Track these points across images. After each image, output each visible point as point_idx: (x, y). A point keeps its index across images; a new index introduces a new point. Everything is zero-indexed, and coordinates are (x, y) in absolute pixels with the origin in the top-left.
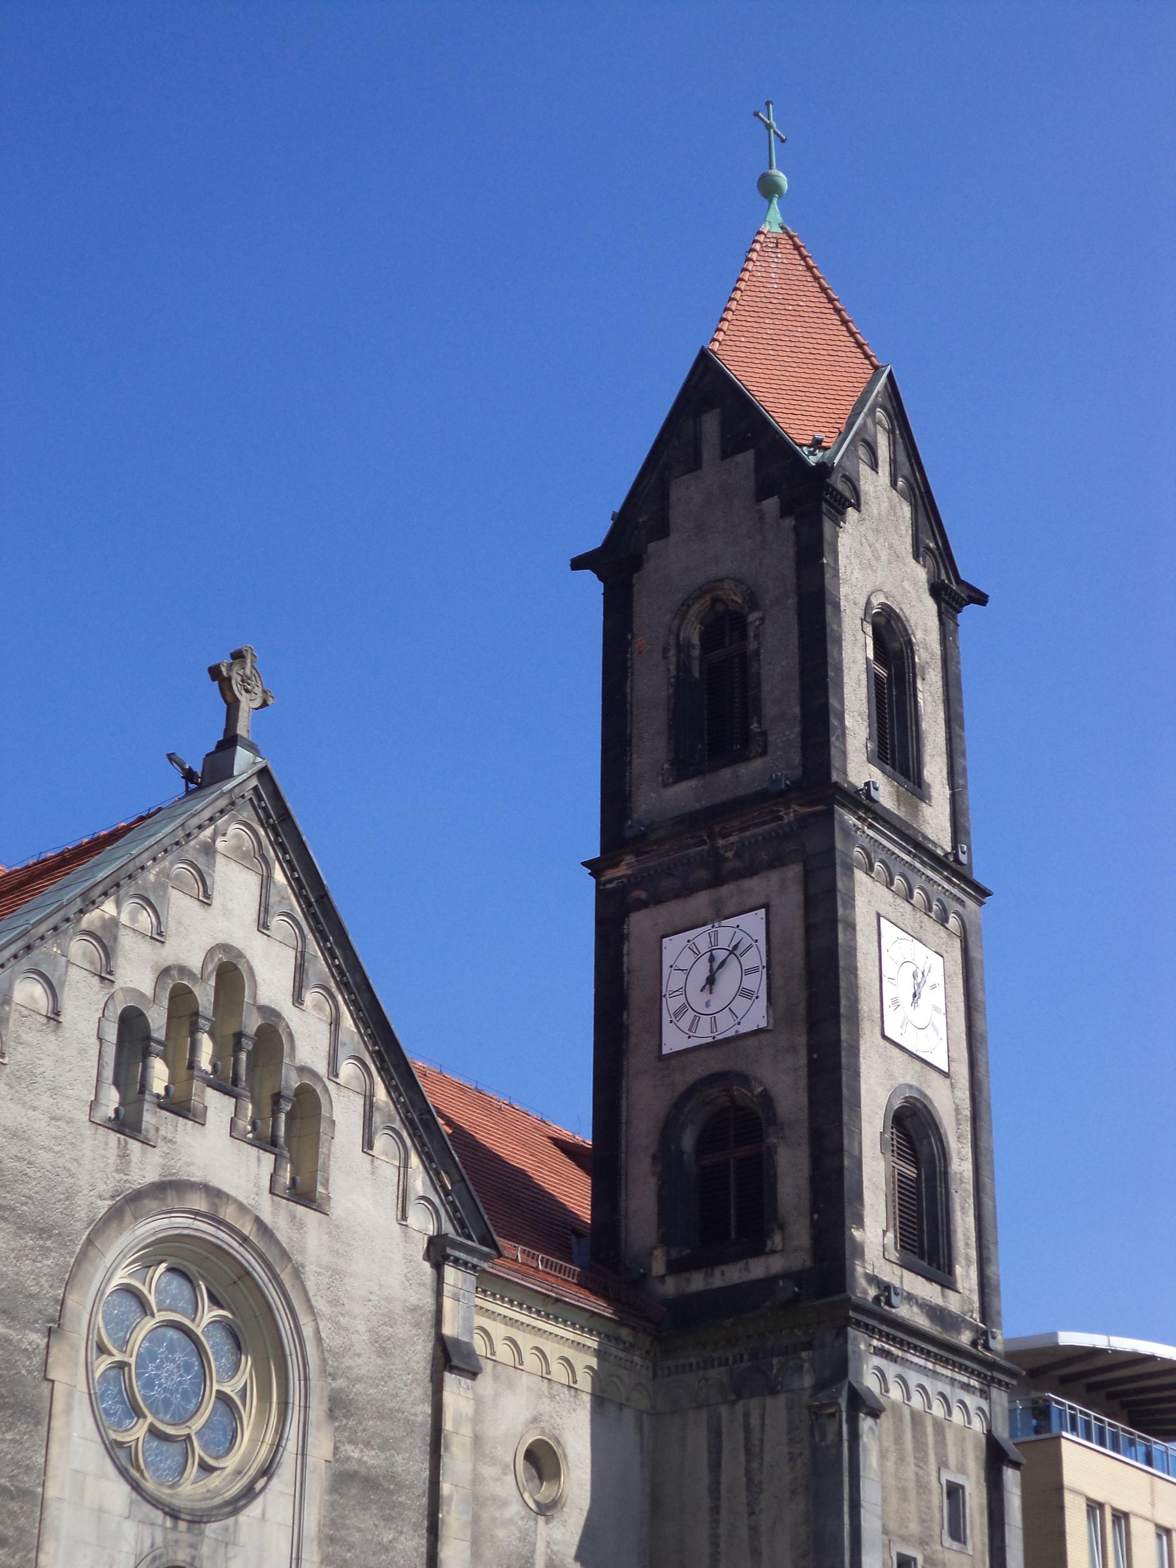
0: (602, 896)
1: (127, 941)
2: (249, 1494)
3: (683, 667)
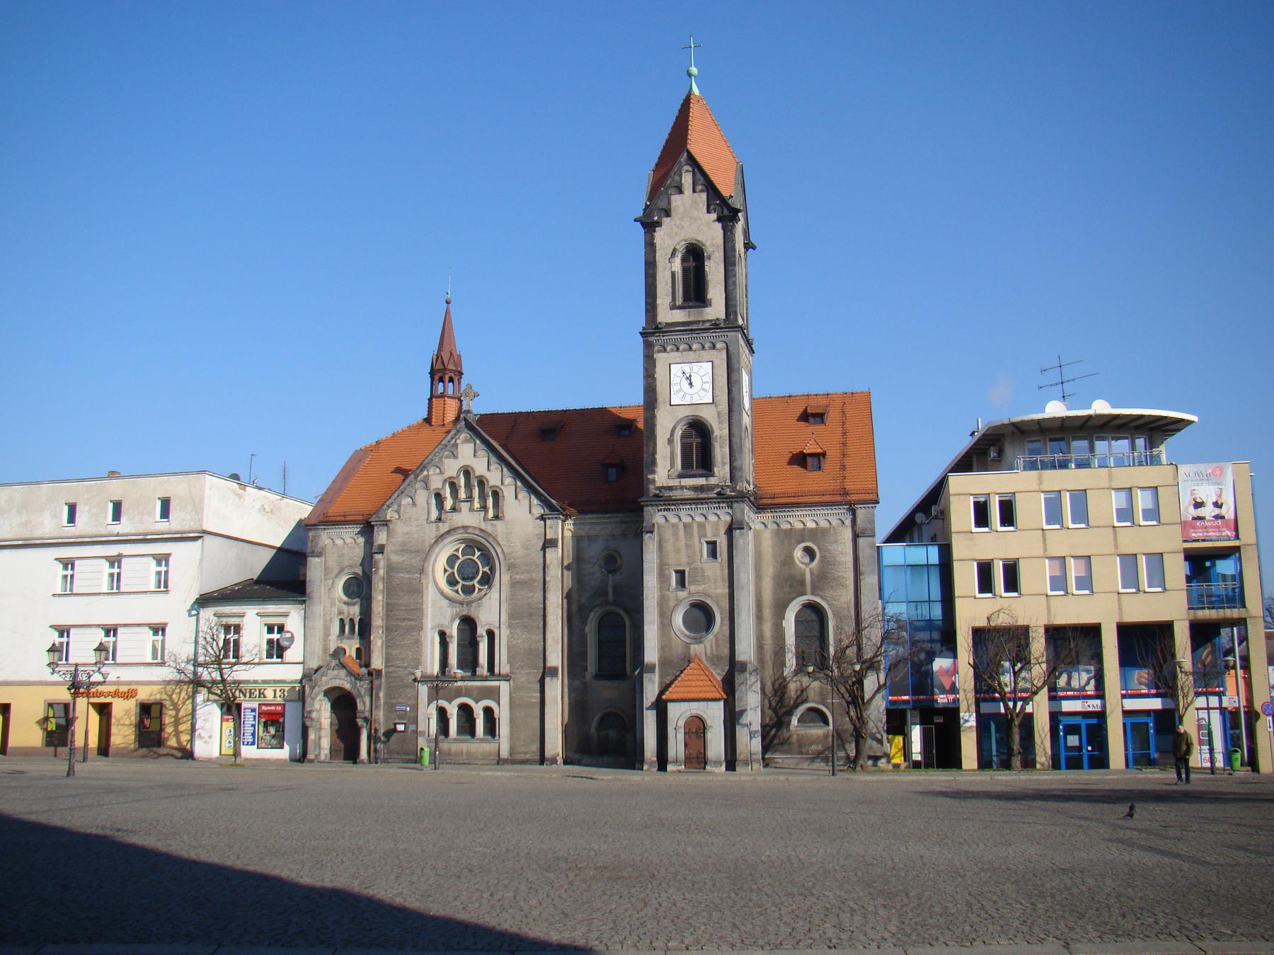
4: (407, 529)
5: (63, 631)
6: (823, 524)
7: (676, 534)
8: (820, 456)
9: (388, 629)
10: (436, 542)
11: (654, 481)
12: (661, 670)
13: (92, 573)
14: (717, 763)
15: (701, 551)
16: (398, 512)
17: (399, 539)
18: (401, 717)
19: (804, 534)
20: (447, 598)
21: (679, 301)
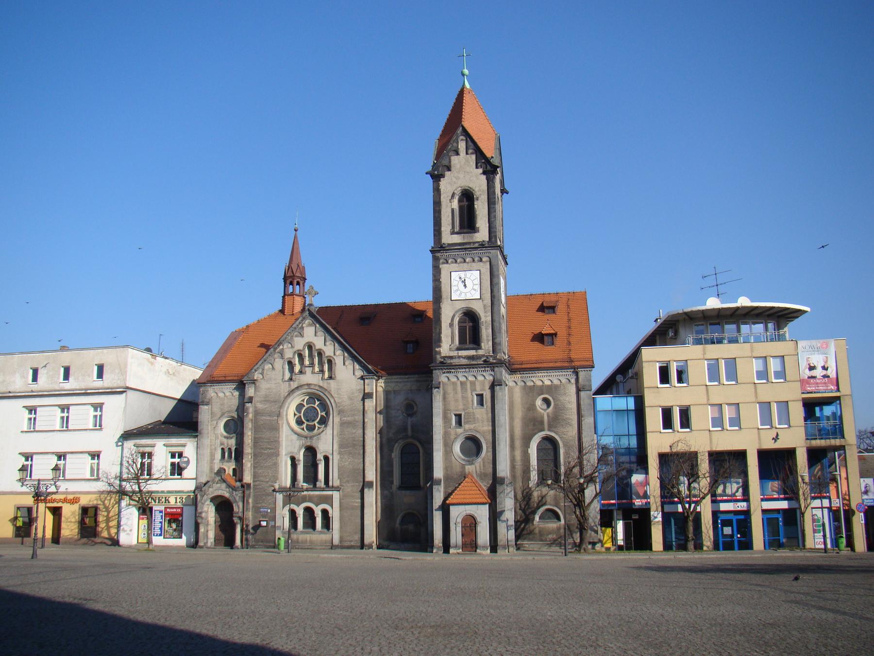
4: (268, 386)
5: (28, 456)
6: (556, 382)
7: (455, 389)
8: (553, 335)
9: (255, 455)
10: (289, 395)
11: (440, 353)
12: (445, 483)
13: (50, 416)
14: (484, 547)
15: (473, 401)
16: (262, 374)
18: (264, 516)
19: (542, 390)
20: (296, 433)
21: (457, 229)
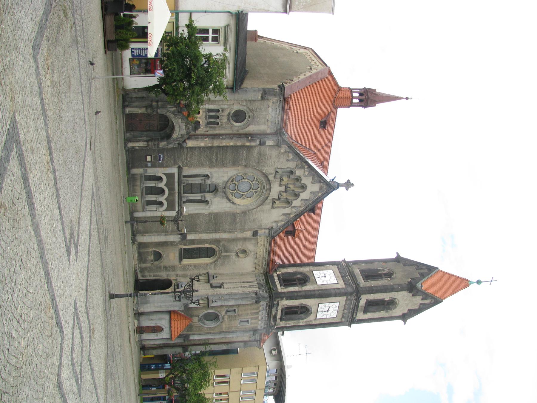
0: (339, 262)
1: (303, 170)
2: (229, 200)
3: (380, 270)
4: (273, 156)
7: (254, 309)
9: (211, 148)
10: (264, 174)
11: (282, 299)
16: (286, 152)
17: (268, 152)
20: (229, 180)
